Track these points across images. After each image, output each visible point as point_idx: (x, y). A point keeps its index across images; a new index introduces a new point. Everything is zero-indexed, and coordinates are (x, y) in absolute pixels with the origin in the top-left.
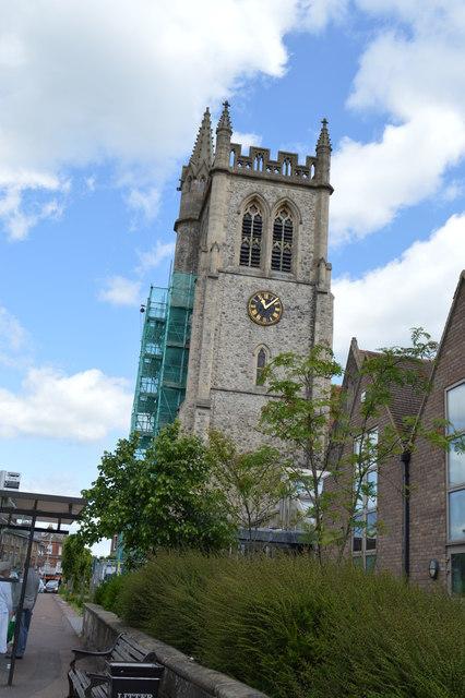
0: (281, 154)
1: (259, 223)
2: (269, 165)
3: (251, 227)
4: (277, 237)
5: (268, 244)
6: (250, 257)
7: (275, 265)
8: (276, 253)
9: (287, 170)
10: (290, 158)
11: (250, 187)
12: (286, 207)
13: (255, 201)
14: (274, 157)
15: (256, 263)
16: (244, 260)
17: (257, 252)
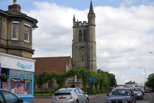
0: (84, 22)
1: (81, 34)
2: (82, 24)
3: (80, 35)
4: (84, 36)
5: (83, 38)
6: (80, 40)
7: (84, 41)
8: (84, 39)
9: (85, 24)
10: (86, 22)
11: (79, 29)
12: (85, 31)
13: (80, 31)
14: (82, 23)
15: (81, 41)
16: (79, 41)
17: (81, 39)
